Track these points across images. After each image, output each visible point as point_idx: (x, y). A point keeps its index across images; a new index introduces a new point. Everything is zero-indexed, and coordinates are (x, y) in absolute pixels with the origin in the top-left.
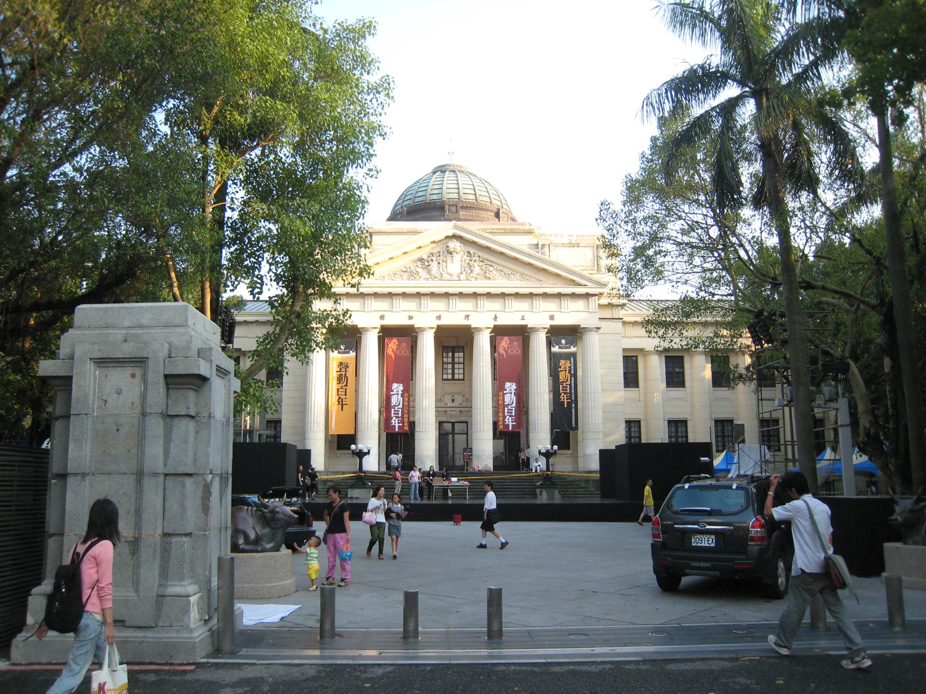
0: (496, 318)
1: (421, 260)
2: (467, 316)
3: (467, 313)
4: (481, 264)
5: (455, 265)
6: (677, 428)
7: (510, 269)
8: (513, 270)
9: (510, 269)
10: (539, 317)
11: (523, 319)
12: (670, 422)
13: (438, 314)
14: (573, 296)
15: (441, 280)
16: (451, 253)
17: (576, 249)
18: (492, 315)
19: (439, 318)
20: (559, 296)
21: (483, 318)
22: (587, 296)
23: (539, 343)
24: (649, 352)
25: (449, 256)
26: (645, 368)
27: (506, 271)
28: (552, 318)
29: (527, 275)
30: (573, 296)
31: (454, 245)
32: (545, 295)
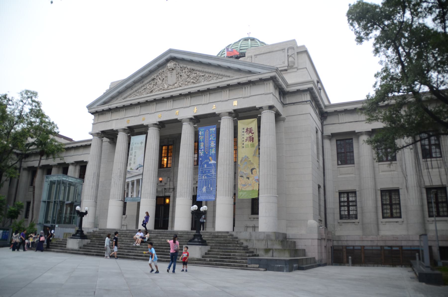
1: (153, 79)
5: (172, 78)
6: (390, 197)
7: (208, 73)
8: (210, 73)
9: (208, 73)
12: (383, 192)
14: (250, 83)
15: (164, 90)
20: (240, 85)
21: (184, 111)
22: (262, 81)
23: (226, 124)
24: (360, 134)
25: (169, 72)
26: (358, 148)
27: (207, 75)
29: (219, 75)
30: (250, 83)
31: (170, 65)
32: (228, 87)
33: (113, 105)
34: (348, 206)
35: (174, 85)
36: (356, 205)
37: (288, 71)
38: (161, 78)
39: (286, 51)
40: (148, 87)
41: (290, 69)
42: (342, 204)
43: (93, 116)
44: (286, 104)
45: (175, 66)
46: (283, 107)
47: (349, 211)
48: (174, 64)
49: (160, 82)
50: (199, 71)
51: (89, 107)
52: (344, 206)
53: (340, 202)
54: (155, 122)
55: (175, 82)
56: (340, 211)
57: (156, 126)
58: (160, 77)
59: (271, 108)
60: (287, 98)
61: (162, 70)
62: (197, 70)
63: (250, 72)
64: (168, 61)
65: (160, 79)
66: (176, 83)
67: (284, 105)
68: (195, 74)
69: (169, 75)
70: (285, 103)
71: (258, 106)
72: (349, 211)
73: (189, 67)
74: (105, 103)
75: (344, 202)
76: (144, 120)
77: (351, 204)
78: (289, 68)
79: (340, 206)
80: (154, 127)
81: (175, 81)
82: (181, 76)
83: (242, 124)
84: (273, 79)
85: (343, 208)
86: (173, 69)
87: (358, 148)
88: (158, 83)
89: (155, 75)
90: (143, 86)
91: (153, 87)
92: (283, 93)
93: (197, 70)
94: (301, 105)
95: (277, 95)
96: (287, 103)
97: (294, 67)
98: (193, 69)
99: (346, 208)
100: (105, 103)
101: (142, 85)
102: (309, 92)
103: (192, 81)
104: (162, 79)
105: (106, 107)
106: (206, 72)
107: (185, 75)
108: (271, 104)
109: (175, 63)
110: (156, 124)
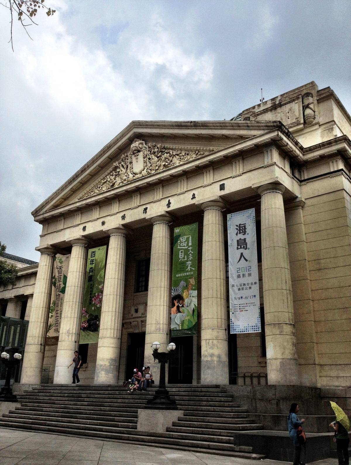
0: (169, 203)
1: (116, 167)
2: (146, 209)
3: (145, 207)
4: (160, 154)
5: (138, 165)
10: (206, 191)
11: (194, 197)
13: (122, 214)
16: (134, 154)
17: (279, 110)
18: (166, 202)
19: (123, 217)
23: (211, 220)
25: (133, 156)
28: (222, 187)
35: (141, 173)
38: (124, 165)
40: (109, 180)
43: (41, 226)
44: (305, 180)
45: (140, 146)
46: (300, 186)
48: (139, 144)
49: (124, 171)
50: (172, 149)
51: (35, 213)
54: (118, 226)
55: (142, 168)
58: (122, 163)
60: (305, 172)
61: (126, 154)
62: (169, 149)
64: (131, 140)
65: (123, 166)
66: (143, 170)
67: (301, 182)
68: (167, 153)
70: (303, 179)
73: (159, 146)
74: (56, 207)
76: (103, 223)
80: (118, 232)
81: (142, 168)
82: (149, 159)
83: (236, 219)
84: (275, 143)
88: (120, 172)
89: (117, 163)
90: (104, 179)
91: (115, 179)
92: (297, 165)
93: (169, 149)
94: (329, 178)
95: (288, 168)
96: (306, 178)
97: (314, 122)
98: (164, 148)
100: (56, 207)
102: (339, 157)
103: (163, 163)
104: (125, 166)
106: (181, 150)
107: (153, 157)
109: (141, 142)
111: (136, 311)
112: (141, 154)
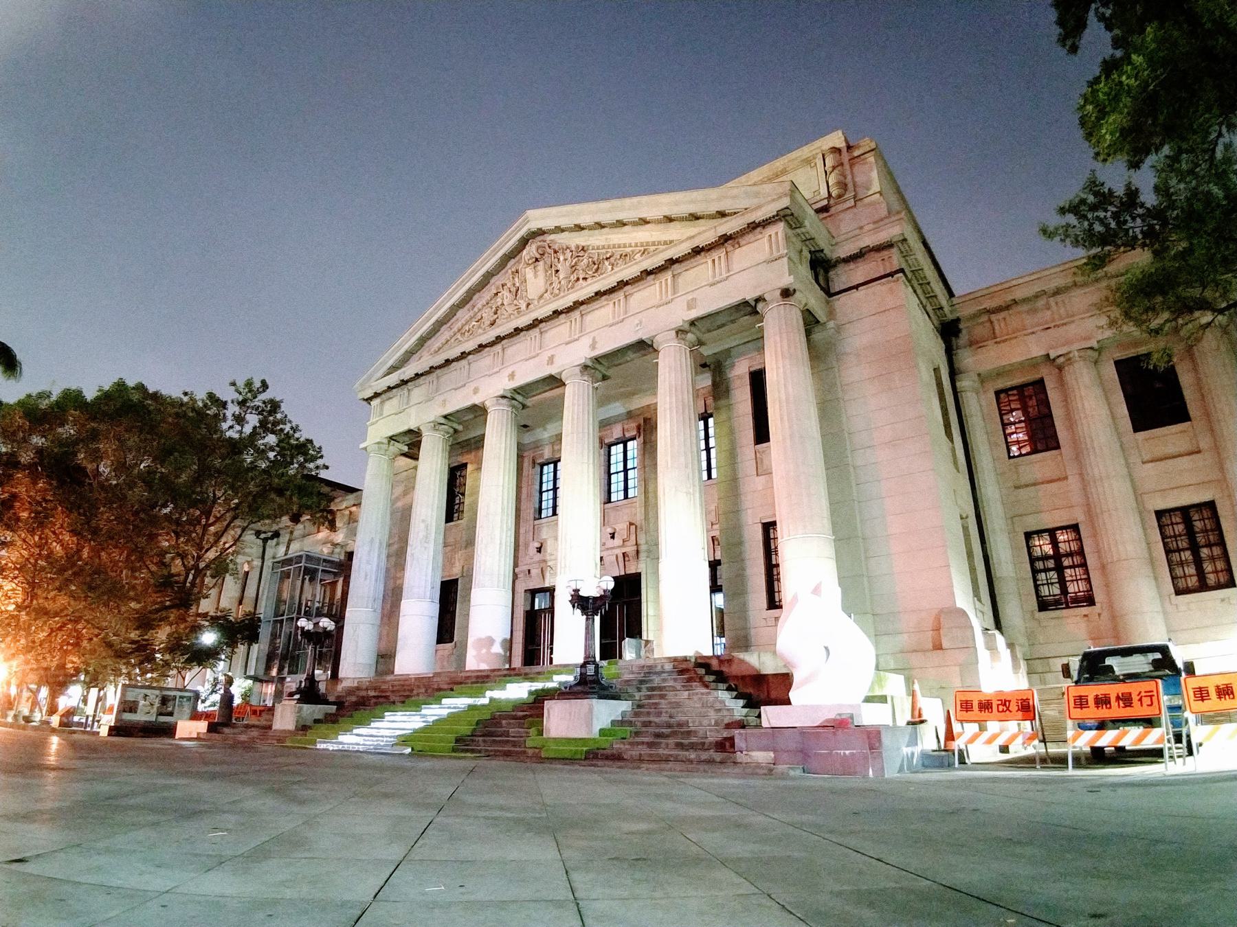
28: (690, 306)
33: (408, 372)
34: (1060, 569)
35: (541, 297)
36: (1084, 565)
37: (833, 210)
39: (820, 162)
41: (836, 204)
42: (1040, 565)
47: (1062, 582)
52: (1046, 570)
53: (1033, 560)
54: (501, 393)
55: (543, 290)
56: (1036, 587)
57: (505, 401)
59: (786, 293)
63: (722, 214)
69: (529, 273)
71: (750, 296)
72: (1062, 582)
75: (1045, 558)
76: (476, 391)
77: (1066, 562)
78: (832, 202)
79: (1035, 572)
85: (1042, 576)
86: (537, 260)
87: (1066, 400)
92: (821, 266)
99: (1053, 575)
100: (394, 369)
101: (472, 313)
104: (513, 290)
105: (393, 379)
108: (787, 281)
110: (503, 397)
111: (539, 550)
112: (541, 263)
